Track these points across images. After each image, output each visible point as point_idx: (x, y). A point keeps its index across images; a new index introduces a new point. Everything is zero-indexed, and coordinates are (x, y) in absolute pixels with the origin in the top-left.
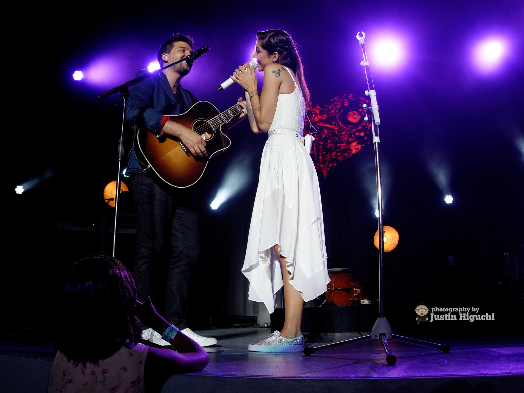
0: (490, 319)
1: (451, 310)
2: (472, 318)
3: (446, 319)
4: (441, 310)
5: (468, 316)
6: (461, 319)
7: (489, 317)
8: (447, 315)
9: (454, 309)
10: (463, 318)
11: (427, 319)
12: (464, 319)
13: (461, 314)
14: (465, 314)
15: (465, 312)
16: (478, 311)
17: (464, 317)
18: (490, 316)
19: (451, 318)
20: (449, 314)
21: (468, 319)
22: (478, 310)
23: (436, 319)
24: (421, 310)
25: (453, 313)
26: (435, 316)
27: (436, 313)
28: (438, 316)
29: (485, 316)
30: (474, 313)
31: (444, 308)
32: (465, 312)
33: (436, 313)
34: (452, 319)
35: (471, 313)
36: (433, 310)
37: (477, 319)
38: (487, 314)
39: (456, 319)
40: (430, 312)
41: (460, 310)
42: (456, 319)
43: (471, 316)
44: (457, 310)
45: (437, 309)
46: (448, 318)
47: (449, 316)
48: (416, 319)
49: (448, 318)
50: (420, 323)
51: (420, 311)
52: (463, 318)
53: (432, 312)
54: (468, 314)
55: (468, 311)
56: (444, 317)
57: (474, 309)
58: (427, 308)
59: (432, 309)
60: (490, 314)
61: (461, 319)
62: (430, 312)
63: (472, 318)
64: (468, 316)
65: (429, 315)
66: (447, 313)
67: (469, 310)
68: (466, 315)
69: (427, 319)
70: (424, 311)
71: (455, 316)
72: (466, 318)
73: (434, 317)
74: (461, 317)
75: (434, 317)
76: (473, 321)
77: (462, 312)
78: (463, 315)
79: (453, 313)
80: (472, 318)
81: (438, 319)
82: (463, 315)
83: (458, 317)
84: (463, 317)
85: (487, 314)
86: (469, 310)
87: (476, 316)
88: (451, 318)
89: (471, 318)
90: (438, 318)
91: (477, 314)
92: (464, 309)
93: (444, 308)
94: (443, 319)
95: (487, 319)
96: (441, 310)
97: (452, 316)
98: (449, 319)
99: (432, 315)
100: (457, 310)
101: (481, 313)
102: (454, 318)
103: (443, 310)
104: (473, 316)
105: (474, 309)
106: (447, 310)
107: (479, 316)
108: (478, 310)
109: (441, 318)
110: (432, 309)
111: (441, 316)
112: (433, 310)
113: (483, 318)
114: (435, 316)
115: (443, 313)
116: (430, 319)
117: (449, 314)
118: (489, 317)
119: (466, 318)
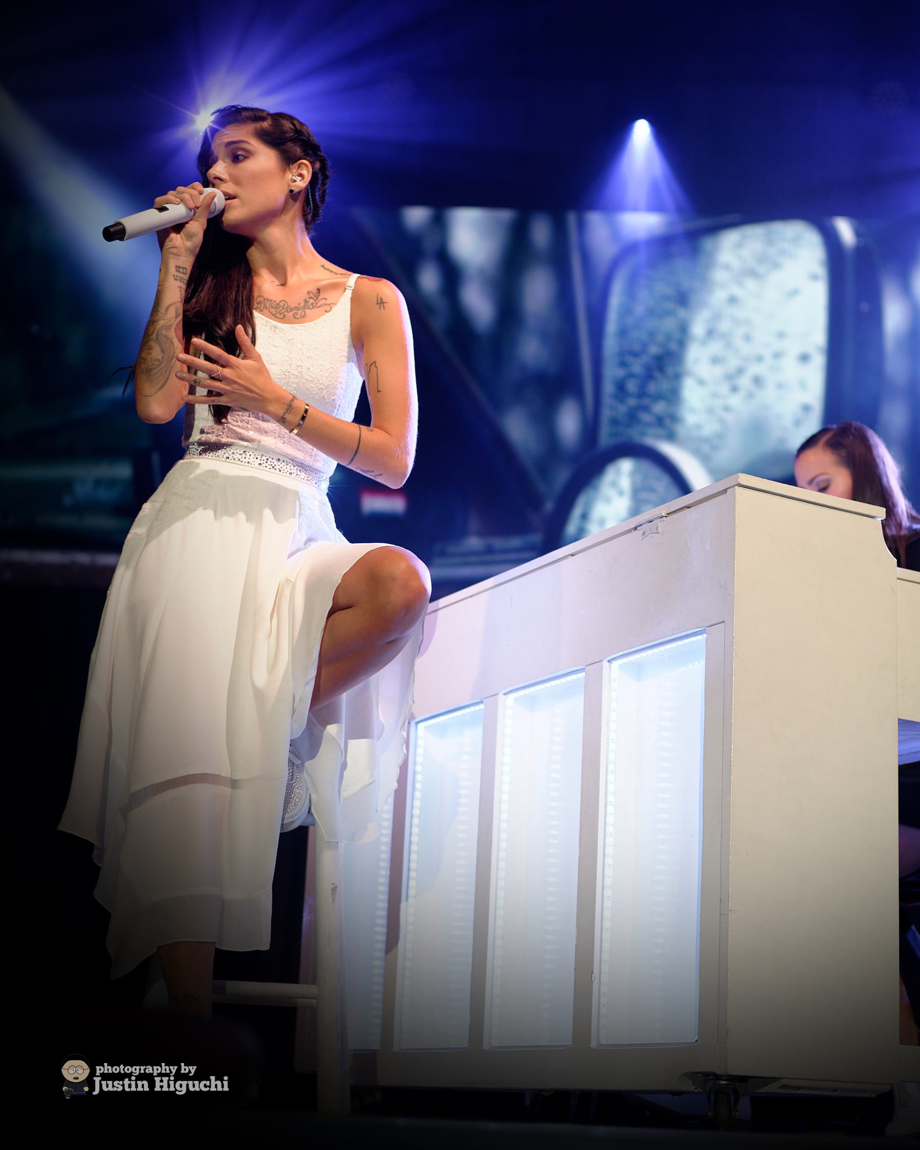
1: (136, 1070)
4: (116, 1070)
9: (143, 1068)
15: (168, 1075)
16: (193, 1071)
24: (75, 1070)
31: (122, 1067)
32: (168, 1075)
40: (93, 1073)
41: (156, 1070)
44: (149, 1070)
45: (107, 1069)
53: (98, 1073)
57: (184, 1069)
59: (98, 1068)
62: (93, 1073)
66: (129, 1076)
67: (174, 1069)
70: (80, 1071)
86: (174, 1069)
92: (165, 1068)
93: (122, 1067)
96: (116, 1070)
100: (149, 1070)
101: (200, 1076)
103: (120, 1069)
105: (184, 1069)
106: (129, 1069)
110: (98, 1068)
112: (99, 1070)
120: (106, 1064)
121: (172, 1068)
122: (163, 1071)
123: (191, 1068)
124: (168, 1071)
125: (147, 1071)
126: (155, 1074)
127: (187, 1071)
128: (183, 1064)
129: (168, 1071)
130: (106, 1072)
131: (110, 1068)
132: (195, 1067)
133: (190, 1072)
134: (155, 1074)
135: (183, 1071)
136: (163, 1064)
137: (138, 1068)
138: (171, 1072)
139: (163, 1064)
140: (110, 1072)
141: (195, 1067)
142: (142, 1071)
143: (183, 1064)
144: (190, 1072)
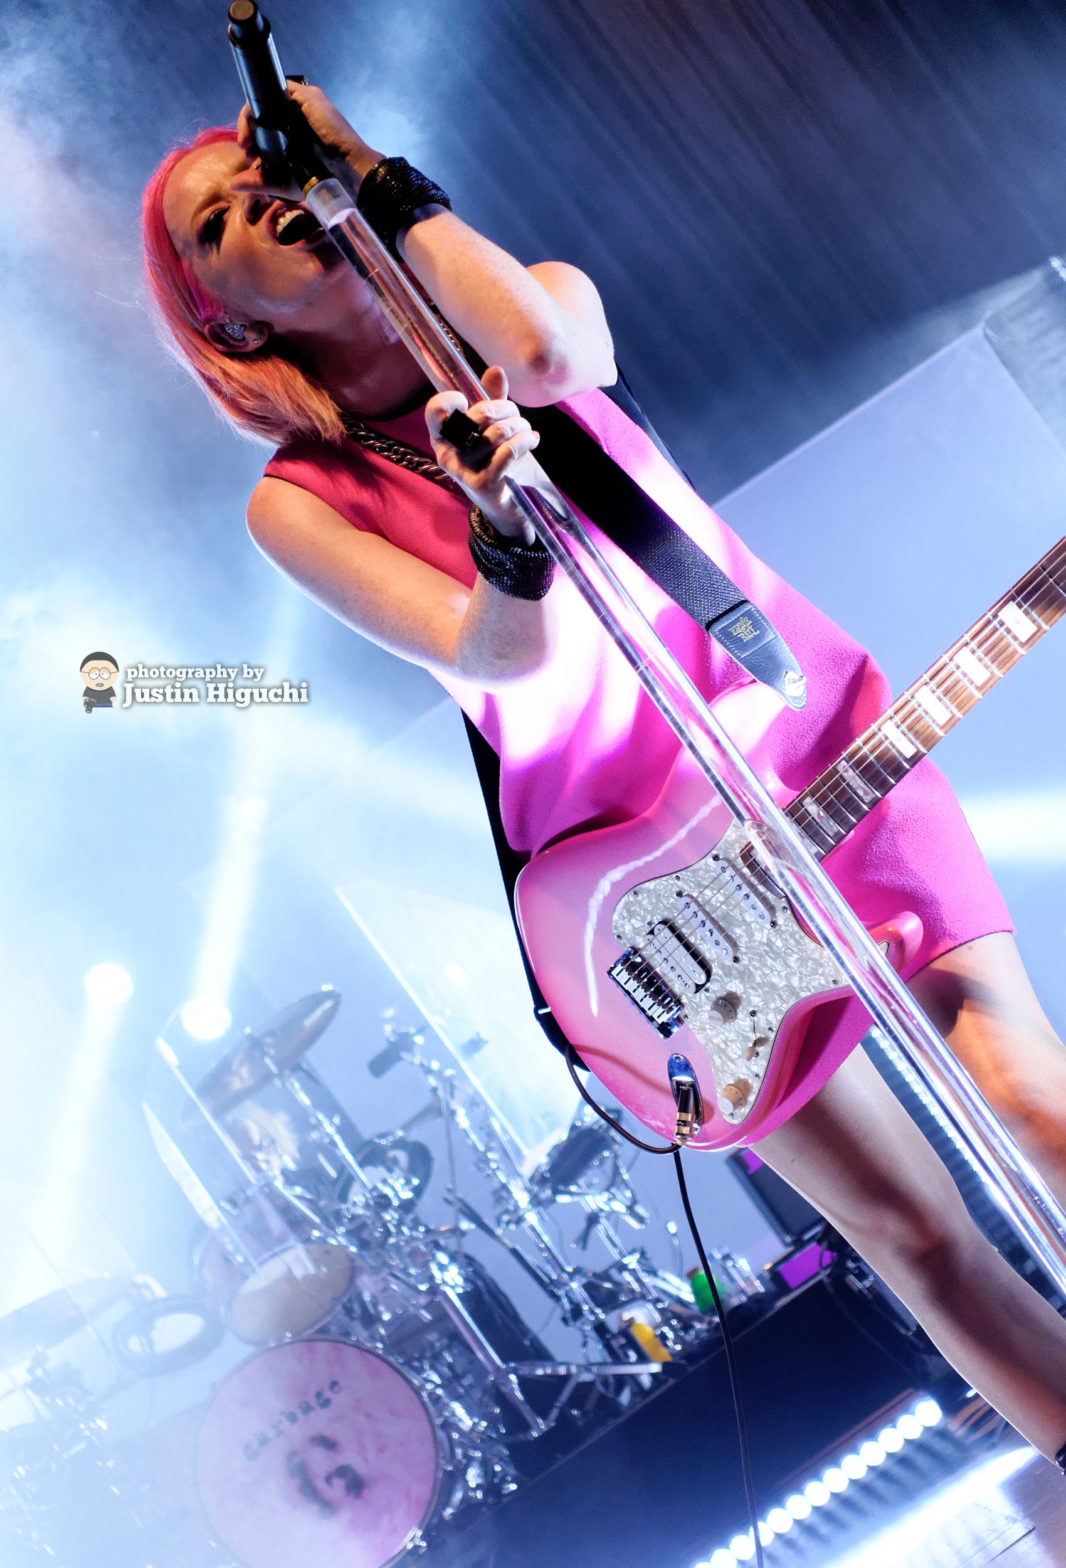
5: (230, 692)
10: (216, 696)
15: (222, 680)
17: (221, 693)
18: (295, 692)
19: (182, 696)
32: (222, 680)
38: (286, 685)
46: (173, 695)
47: (178, 692)
49: (173, 695)
52: (216, 696)
53: (130, 676)
56: (164, 695)
63: (243, 695)
64: (230, 692)
70: (106, 675)
72: (226, 696)
73: (134, 694)
74: (212, 693)
75: (134, 694)
77: (212, 680)
78: (216, 689)
80: (243, 695)
82: (216, 689)
85: (286, 685)
88: (182, 696)
93: (162, 670)
110: (130, 671)
113: (276, 695)
114: (138, 692)
119: (226, 696)
123: (256, 670)
126: (208, 679)
128: (245, 666)
129: (225, 675)
131: (146, 670)
133: (255, 676)
134: (208, 679)
135: (245, 675)
137: (184, 671)
143: (245, 666)
144: (255, 676)
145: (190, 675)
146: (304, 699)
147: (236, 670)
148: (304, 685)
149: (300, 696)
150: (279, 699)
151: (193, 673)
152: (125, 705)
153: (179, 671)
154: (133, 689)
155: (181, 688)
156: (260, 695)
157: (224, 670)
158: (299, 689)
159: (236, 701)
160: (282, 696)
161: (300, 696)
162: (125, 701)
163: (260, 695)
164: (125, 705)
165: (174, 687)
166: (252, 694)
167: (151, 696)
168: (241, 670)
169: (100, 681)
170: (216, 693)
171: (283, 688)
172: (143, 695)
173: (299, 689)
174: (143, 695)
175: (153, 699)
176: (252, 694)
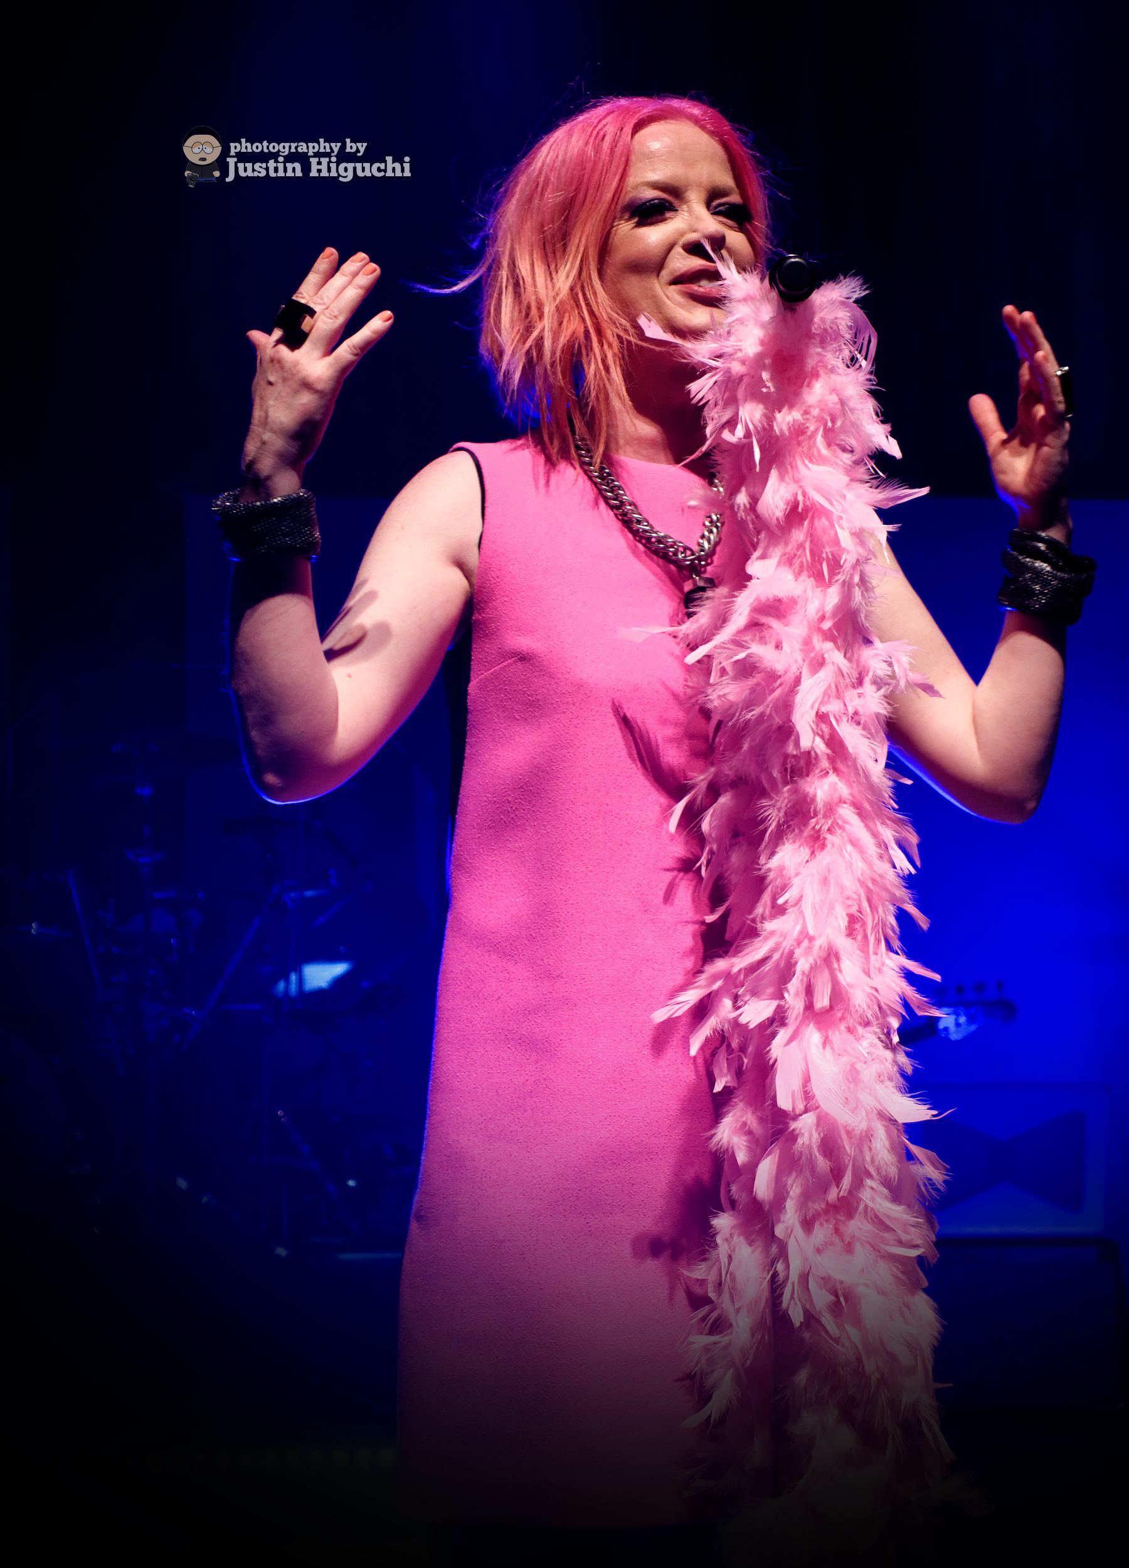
0: (399, 174)
1: (285, 148)
2: (346, 173)
3: (272, 174)
5: (333, 166)
6: (314, 173)
7: (395, 168)
8: (276, 162)
9: (293, 145)
10: (319, 171)
11: (217, 174)
12: (324, 174)
13: (314, 161)
14: (325, 160)
15: (327, 155)
16: (362, 150)
17: (324, 167)
18: (397, 166)
19: (285, 170)
20: (281, 159)
21: (334, 174)
22: (362, 147)
23: (242, 174)
24: (201, 149)
25: (291, 158)
26: (241, 166)
27: (242, 157)
28: (249, 165)
29: (382, 166)
30: (352, 158)
31: (265, 143)
32: (327, 155)
33: (242, 157)
34: (290, 174)
35: (344, 157)
36: (234, 147)
37: (360, 174)
38: (389, 159)
39: (299, 174)
40: (226, 152)
41: (311, 148)
42: (299, 174)
43: (342, 166)
44: (303, 147)
45: (245, 146)
46: (276, 170)
47: (281, 166)
48: (187, 173)
49: (276, 170)
50: (198, 185)
51: (196, 150)
52: (319, 171)
53: (232, 153)
54: (334, 159)
55: (336, 150)
56: (267, 169)
57: (351, 147)
58: (215, 142)
59: (232, 145)
60: (398, 159)
61: (314, 173)
62: (226, 152)
63: (346, 170)
64: (333, 166)
65: (221, 163)
66: (275, 156)
67: (336, 147)
68: (330, 162)
69: (217, 174)
70: (209, 150)
71: (298, 166)
72: (329, 170)
73: (237, 169)
75: (237, 169)
76: (350, 178)
77: (318, 155)
78: (319, 163)
79: (291, 158)
80: (346, 170)
81: (250, 173)
82: (319, 163)
83: (306, 168)
84: (319, 169)
85: (389, 159)
86: (336, 147)
87: (359, 166)
88: (285, 170)
89: (342, 172)
90: (248, 171)
91: (362, 160)
92: (323, 146)
93: (265, 143)
94: (263, 173)
95: (389, 174)
97: (289, 166)
98: (281, 174)
99: (232, 161)
100: (303, 147)
101: (371, 157)
102: (295, 170)
104: (350, 166)
105: (351, 147)
106: (274, 147)
107: (367, 165)
108: (362, 147)
109: (258, 170)
110: (232, 145)
111: (257, 166)
112: (234, 147)
113: (379, 170)
115: (263, 157)
116: (225, 172)
117: (281, 159)
118: (395, 168)
119: (329, 170)
120: (243, 140)
121: (333, 145)
122: (322, 150)
123: (359, 145)
124: (328, 150)
125: (299, 150)
126: (311, 154)
127: (354, 150)
128: (348, 140)
129: (328, 150)
130: (244, 150)
131: (249, 145)
132: (365, 145)
133: (358, 151)
134: (311, 154)
136: (322, 140)
137: (287, 145)
138: (332, 151)
139: (322, 140)
140: (250, 150)
141: (365, 145)
142: (293, 150)
143: (348, 140)
144: (358, 151)
145: (293, 150)
146: (407, 174)
147: (339, 145)
148: (407, 159)
149: (403, 170)
150: (382, 174)
151: (296, 148)
152: (228, 180)
153: (282, 145)
154: (236, 163)
155: (285, 162)
156: (363, 170)
157: (327, 145)
158: (402, 162)
159: (339, 175)
160: (385, 171)
161: (403, 170)
162: (227, 176)
163: (363, 170)
164: (228, 180)
165: (276, 161)
166: (355, 169)
167: (254, 170)
168: (344, 146)
169: (203, 155)
170: (319, 167)
171: (385, 162)
172: (245, 170)
173: (402, 162)
174: (245, 170)
175: (256, 174)
176: (355, 169)
